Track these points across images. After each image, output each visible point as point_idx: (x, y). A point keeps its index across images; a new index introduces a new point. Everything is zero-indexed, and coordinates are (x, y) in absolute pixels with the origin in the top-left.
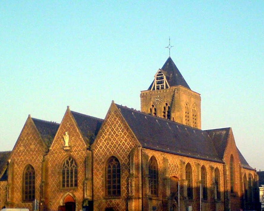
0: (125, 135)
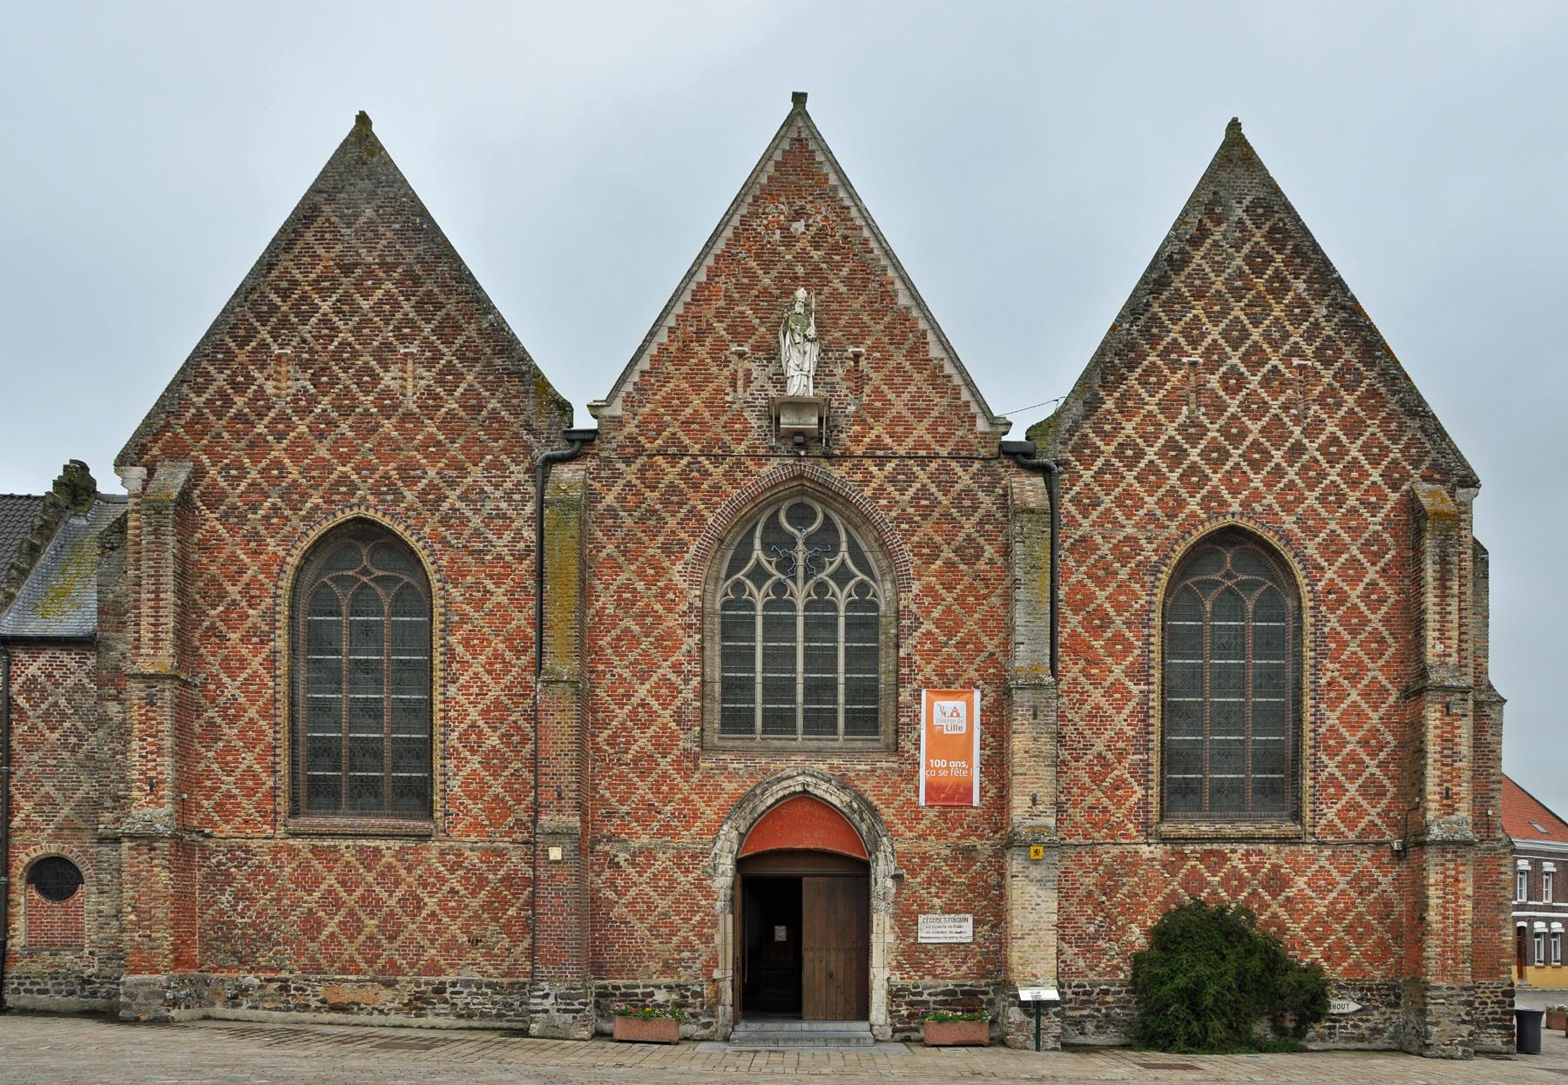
0: (1350, 390)
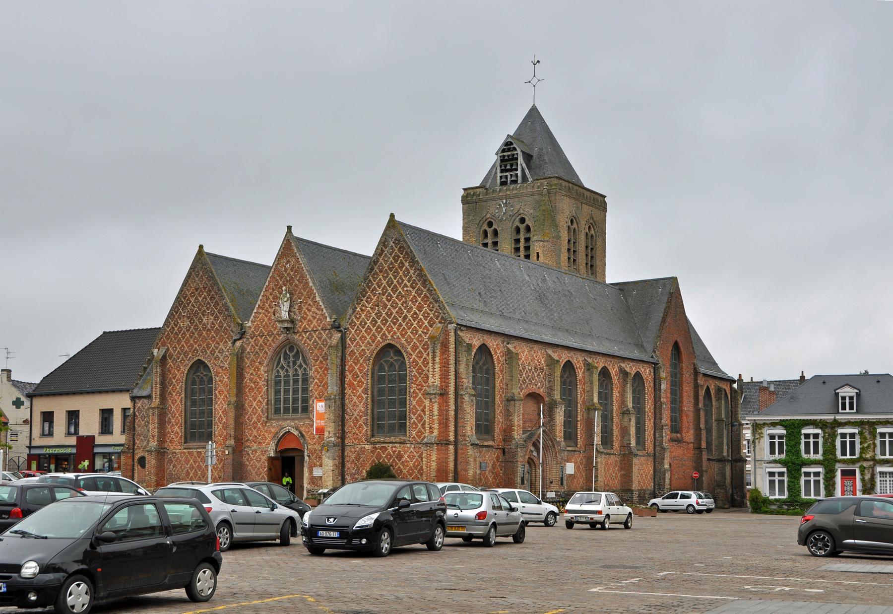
0: (419, 296)
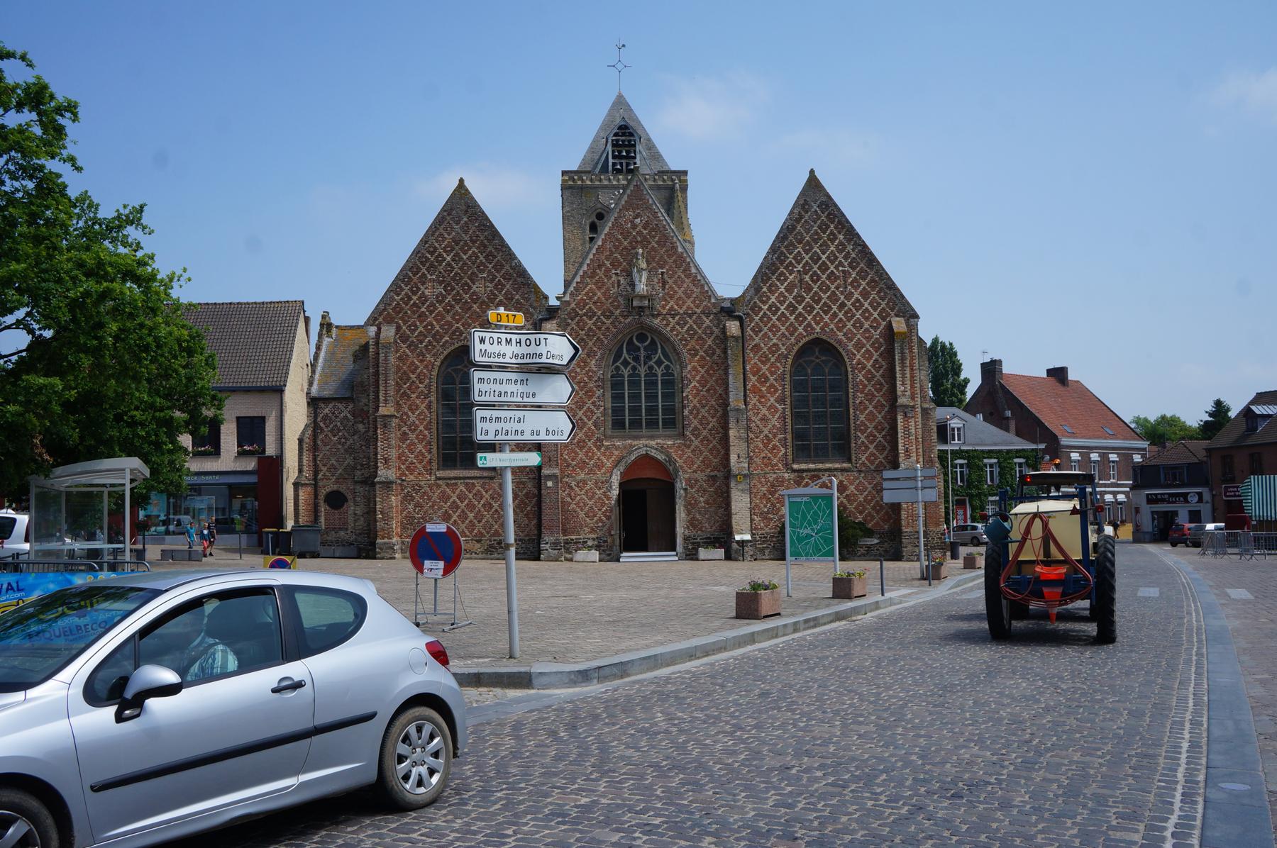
0: (864, 279)
